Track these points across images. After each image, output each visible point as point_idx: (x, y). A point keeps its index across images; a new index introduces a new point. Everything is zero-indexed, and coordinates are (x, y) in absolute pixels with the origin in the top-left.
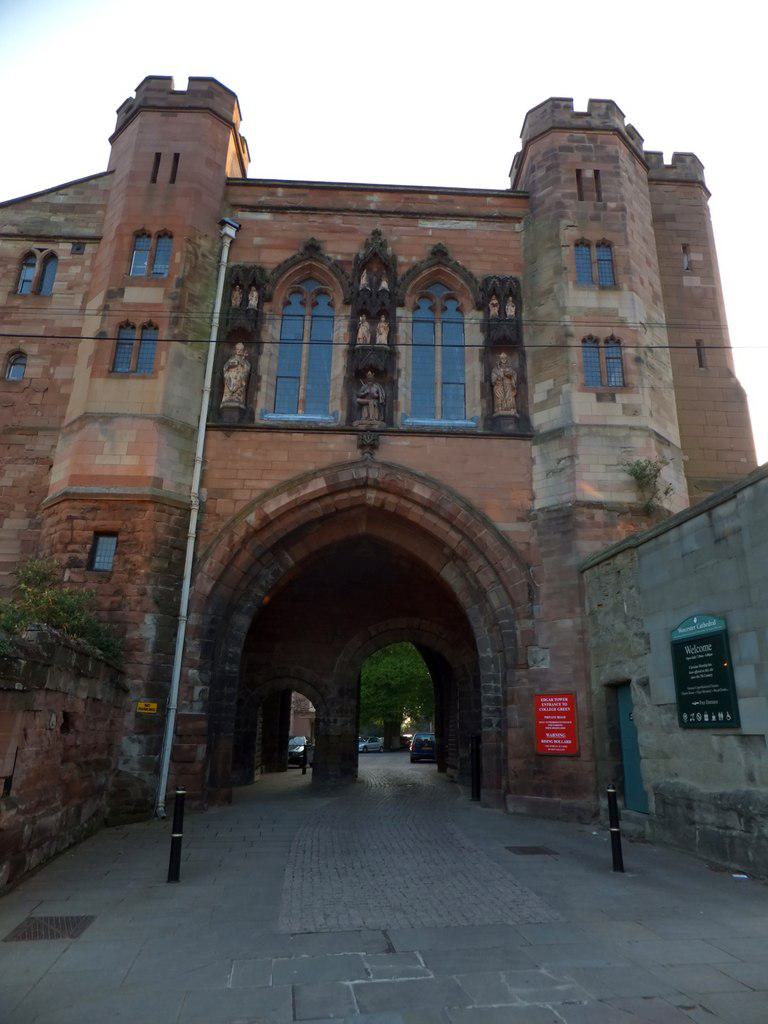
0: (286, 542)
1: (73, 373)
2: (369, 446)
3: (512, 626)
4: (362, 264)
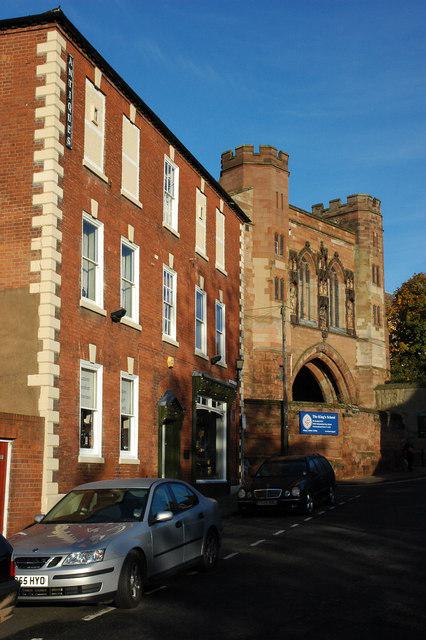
2: (324, 336)
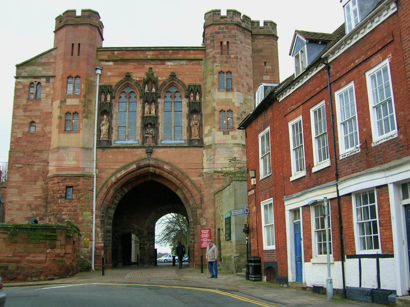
0: (125, 185)
1: (51, 129)
2: (150, 153)
3: (196, 211)
4: (146, 82)
